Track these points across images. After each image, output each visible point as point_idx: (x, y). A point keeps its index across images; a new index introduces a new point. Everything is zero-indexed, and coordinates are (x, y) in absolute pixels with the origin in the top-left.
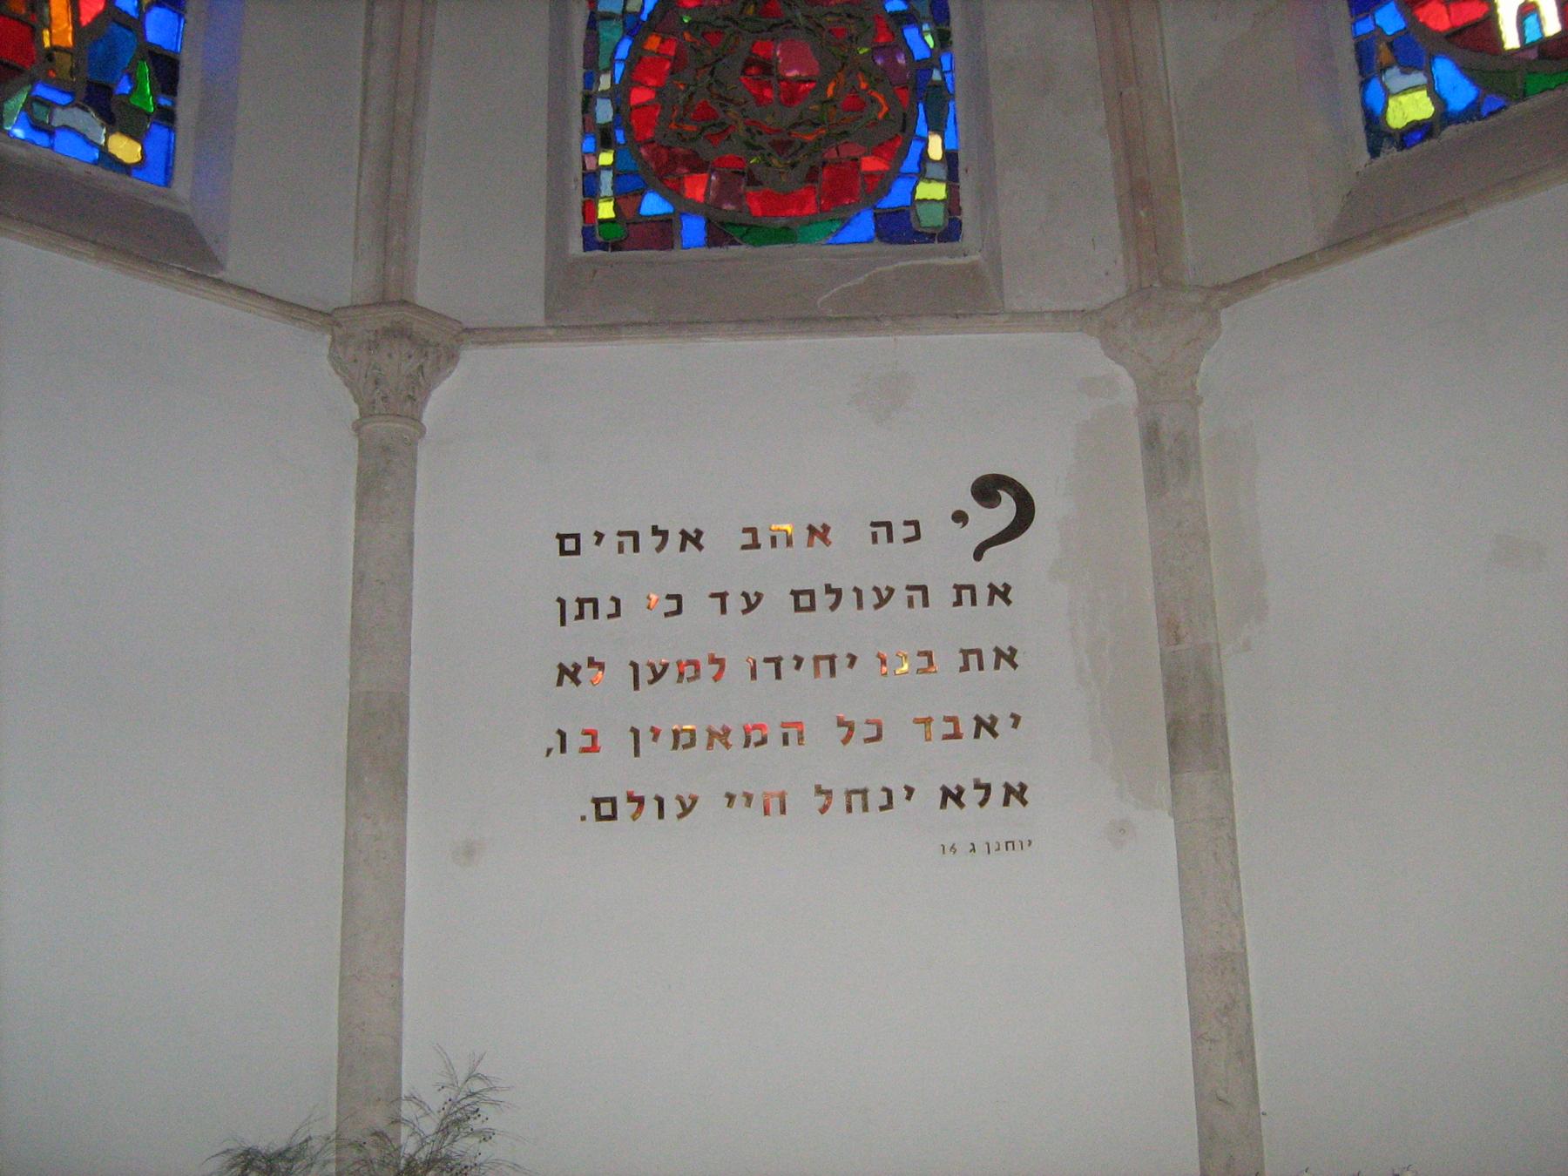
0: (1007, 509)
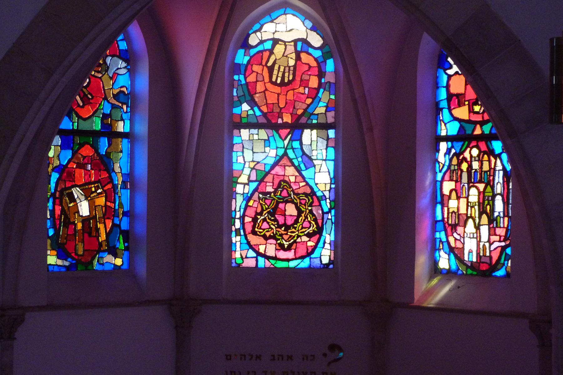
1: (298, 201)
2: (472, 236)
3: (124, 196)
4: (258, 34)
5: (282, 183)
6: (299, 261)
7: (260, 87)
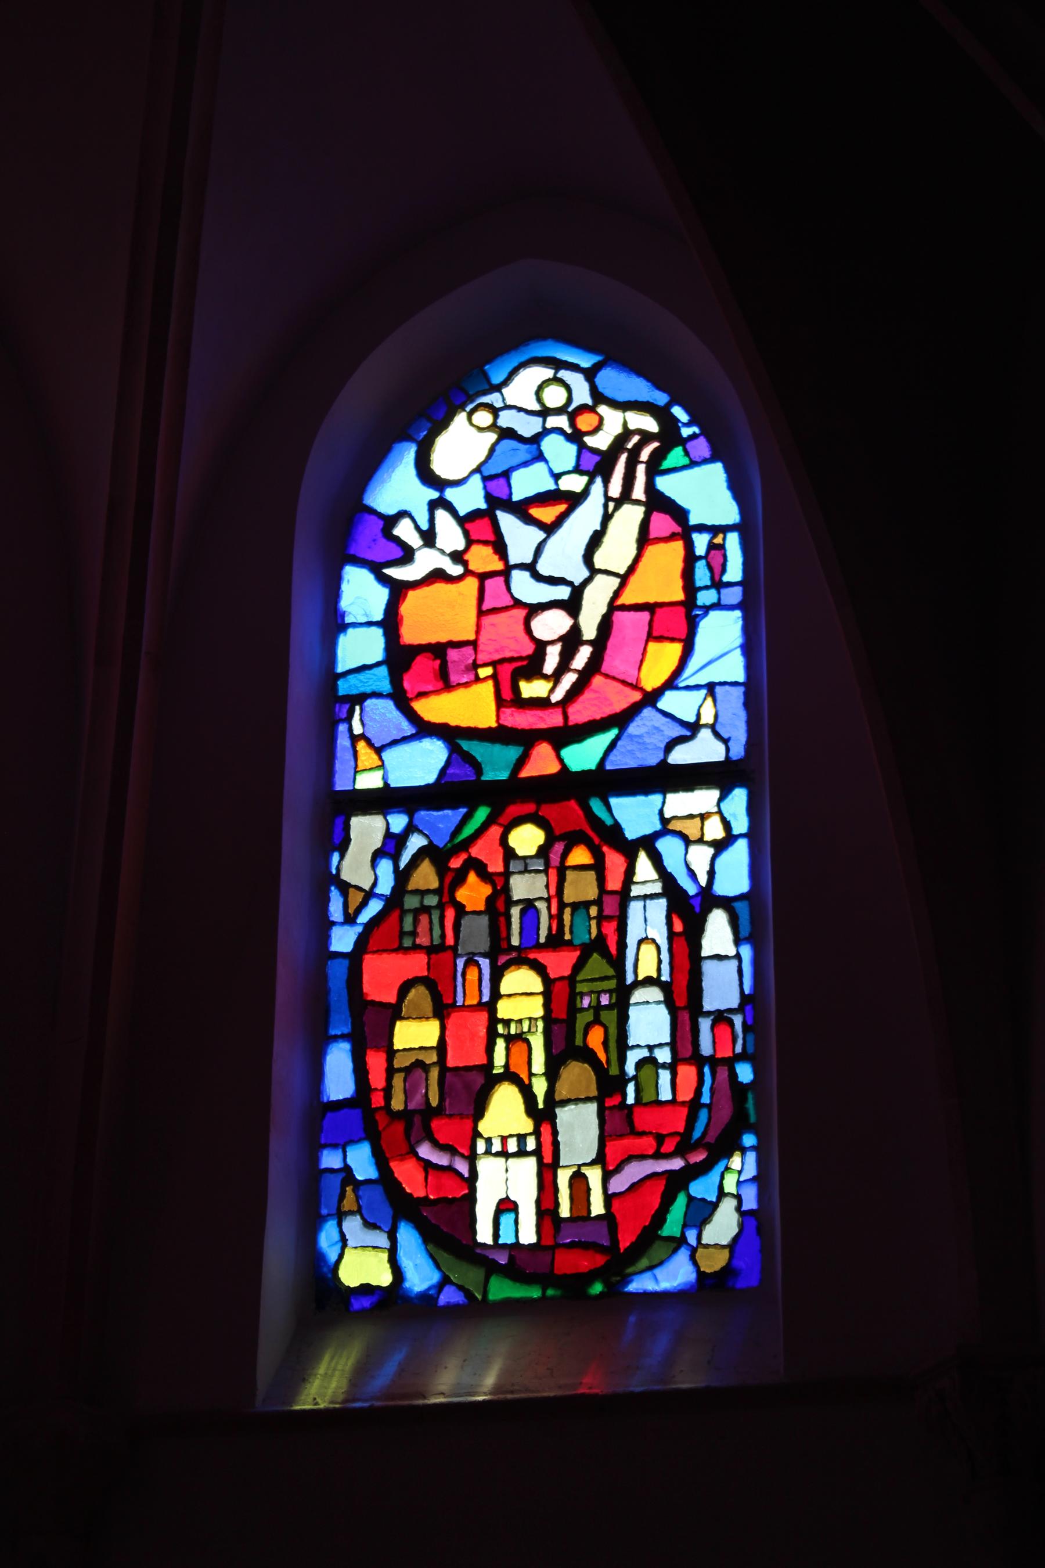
2: (512, 1146)
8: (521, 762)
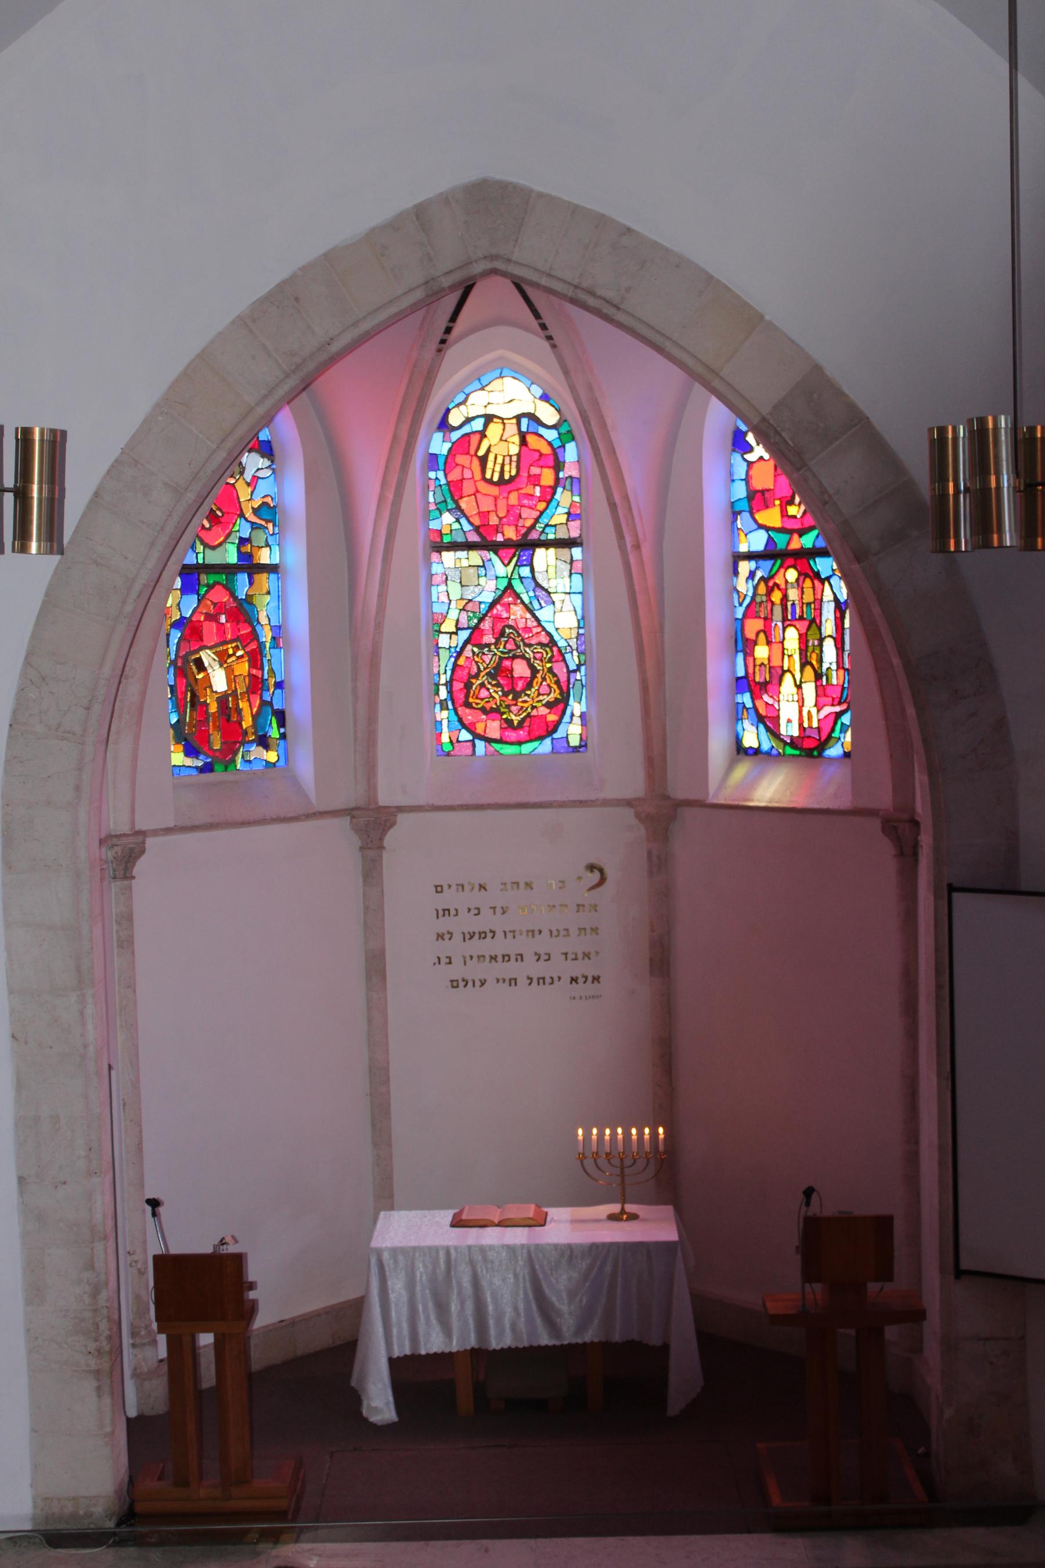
0: (596, 876)
1: (532, 655)
3: (275, 660)
4: (462, 407)
5: (507, 631)
6: (535, 744)
7: (468, 488)
8: (789, 543)
